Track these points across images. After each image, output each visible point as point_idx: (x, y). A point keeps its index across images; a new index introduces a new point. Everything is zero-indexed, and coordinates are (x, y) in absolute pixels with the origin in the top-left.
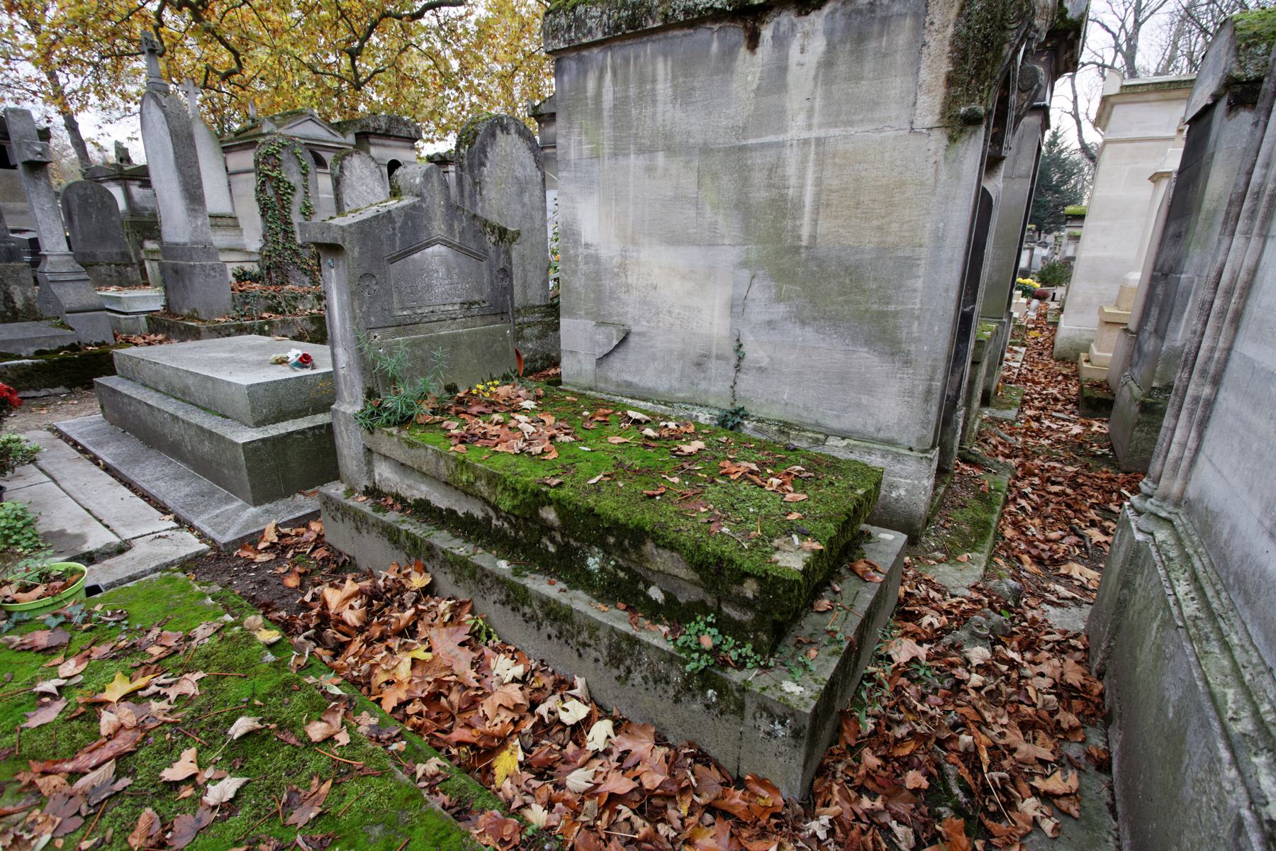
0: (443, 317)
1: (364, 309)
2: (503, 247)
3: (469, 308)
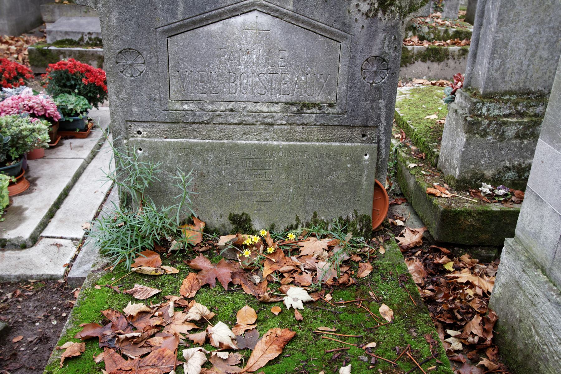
0: (250, 120)
1: (123, 95)
2: (384, 19)
3: (299, 112)
